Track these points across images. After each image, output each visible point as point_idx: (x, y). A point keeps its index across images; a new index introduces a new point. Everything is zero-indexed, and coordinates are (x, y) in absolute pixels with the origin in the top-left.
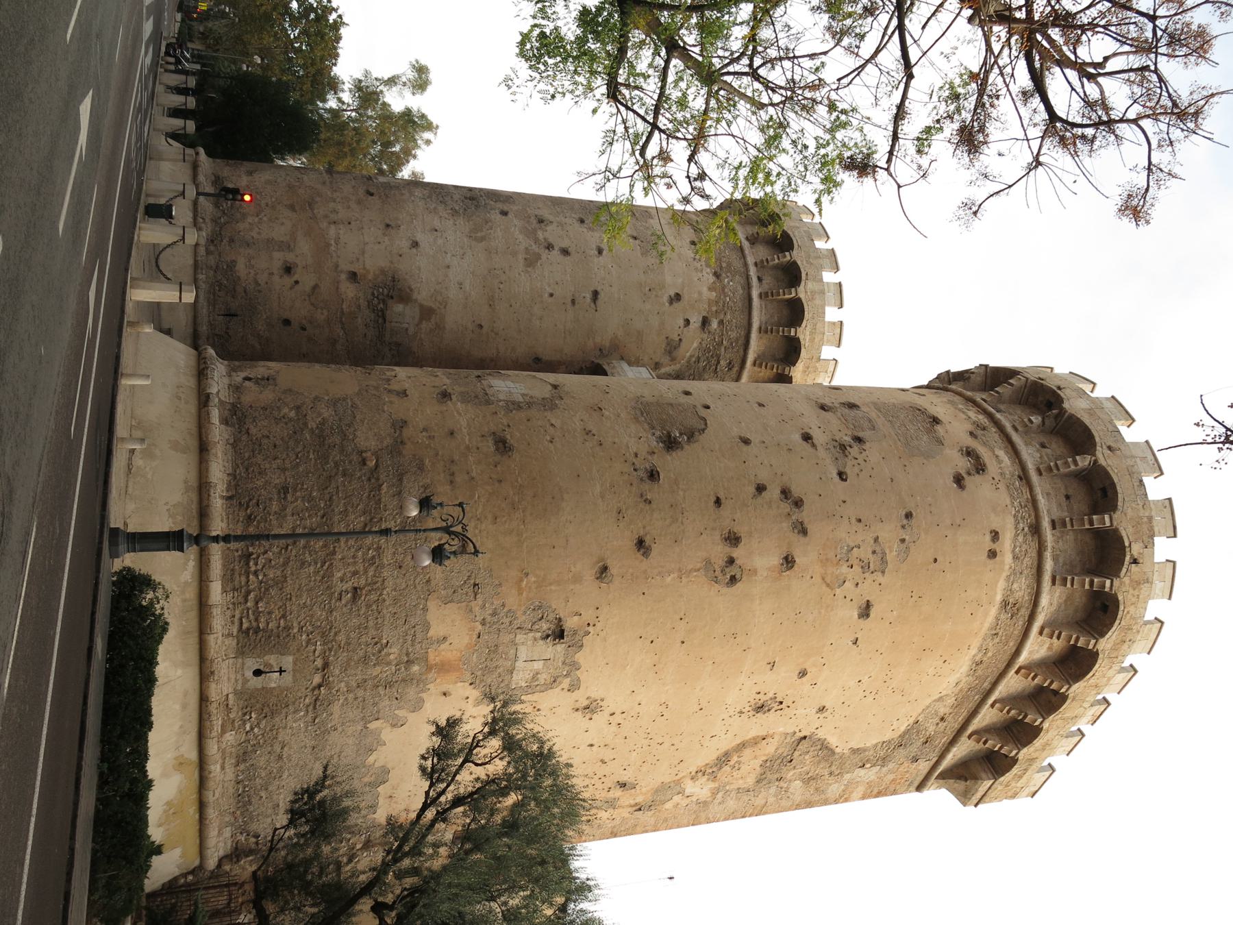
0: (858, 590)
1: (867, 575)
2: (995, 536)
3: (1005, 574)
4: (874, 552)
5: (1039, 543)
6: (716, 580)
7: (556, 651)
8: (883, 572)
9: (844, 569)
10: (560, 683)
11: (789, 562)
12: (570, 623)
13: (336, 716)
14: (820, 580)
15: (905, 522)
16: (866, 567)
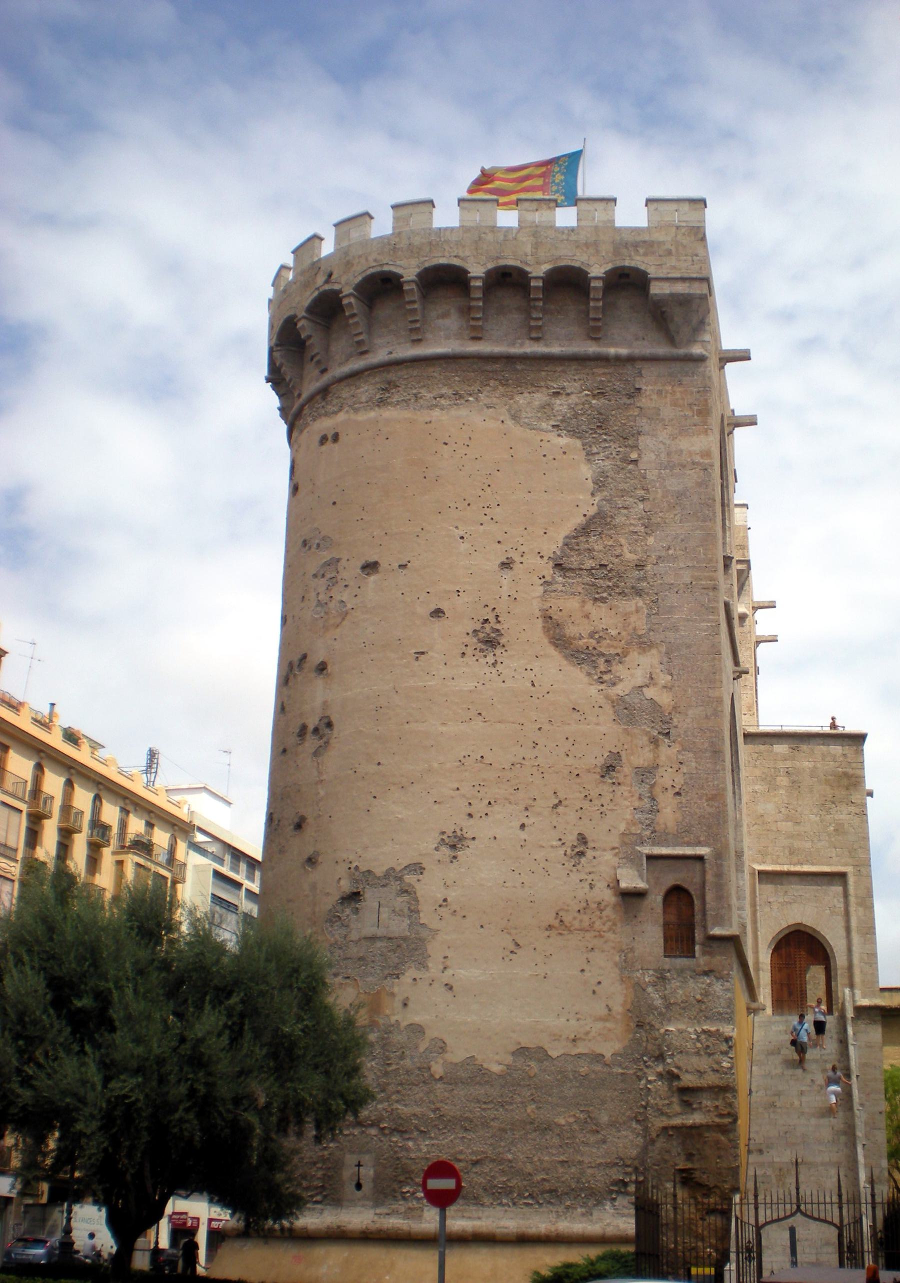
0: (351, 583)
1: (339, 577)
2: (323, 440)
3: (353, 416)
4: (323, 576)
5: (333, 384)
6: (327, 743)
7: (371, 897)
8: (338, 560)
9: (332, 605)
10: (410, 885)
11: (322, 668)
12: (346, 886)
13: (418, 1110)
14: (338, 630)
15: (307, 547)
16: (333, 581)
